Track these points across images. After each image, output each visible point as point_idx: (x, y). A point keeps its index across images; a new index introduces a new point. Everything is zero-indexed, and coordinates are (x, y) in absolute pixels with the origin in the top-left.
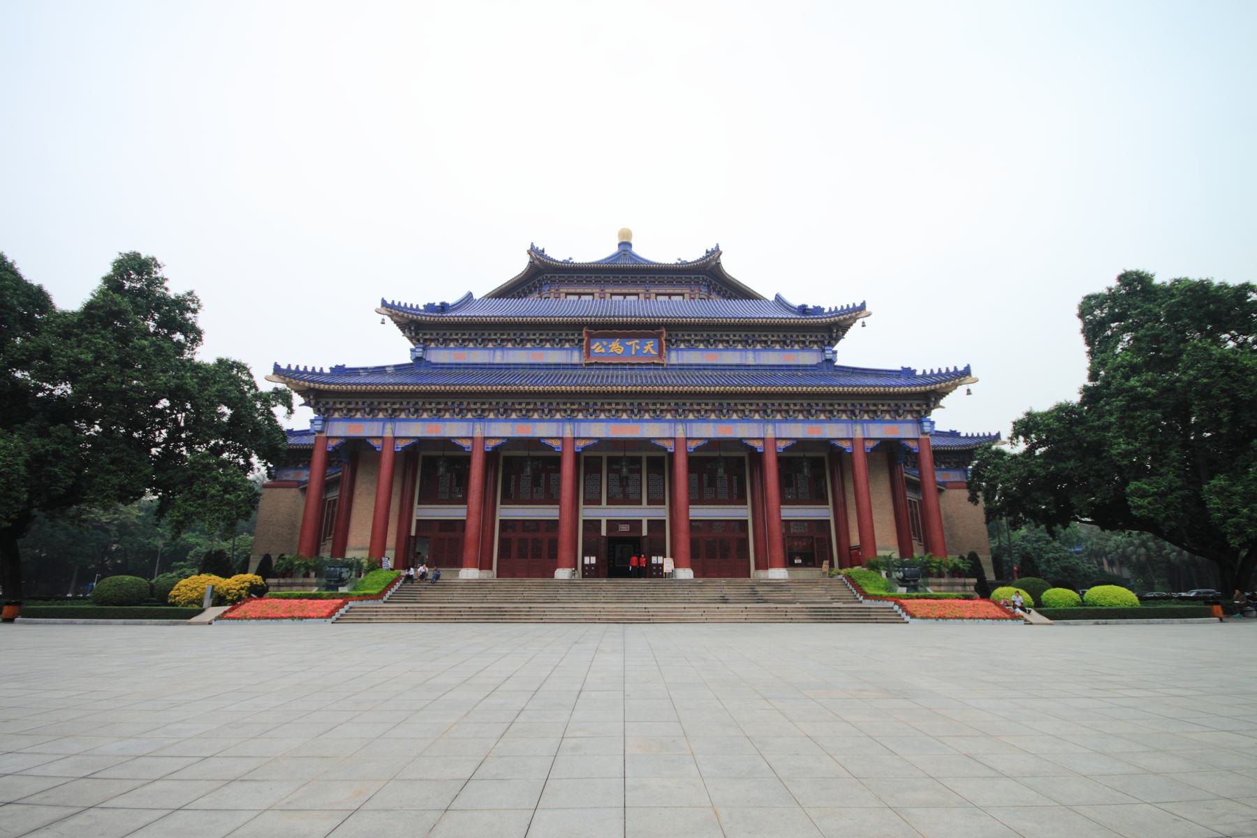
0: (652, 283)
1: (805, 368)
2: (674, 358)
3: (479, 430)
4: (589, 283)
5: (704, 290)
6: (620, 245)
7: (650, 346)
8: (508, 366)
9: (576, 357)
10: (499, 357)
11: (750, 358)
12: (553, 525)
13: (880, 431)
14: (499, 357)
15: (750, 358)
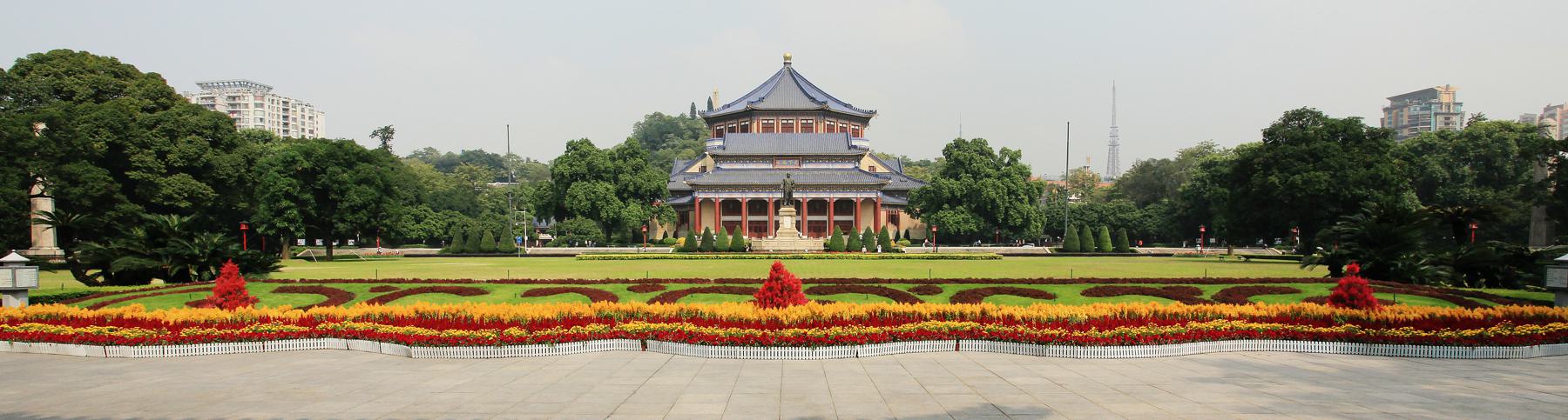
0: (800, 115)
1: (849, 170)
2: (804, 166)
3: (744, 196)
4: (772, 115)
5: (822, 118)
6: (785, 63)
7: (796, 162)
8: (748, 170)
9: (771, 167)
10: (745, 166)
11: (830, 166)
12: (766, 222)
13: (865, 195)
14: (745, 166)
15: (830, 166)
